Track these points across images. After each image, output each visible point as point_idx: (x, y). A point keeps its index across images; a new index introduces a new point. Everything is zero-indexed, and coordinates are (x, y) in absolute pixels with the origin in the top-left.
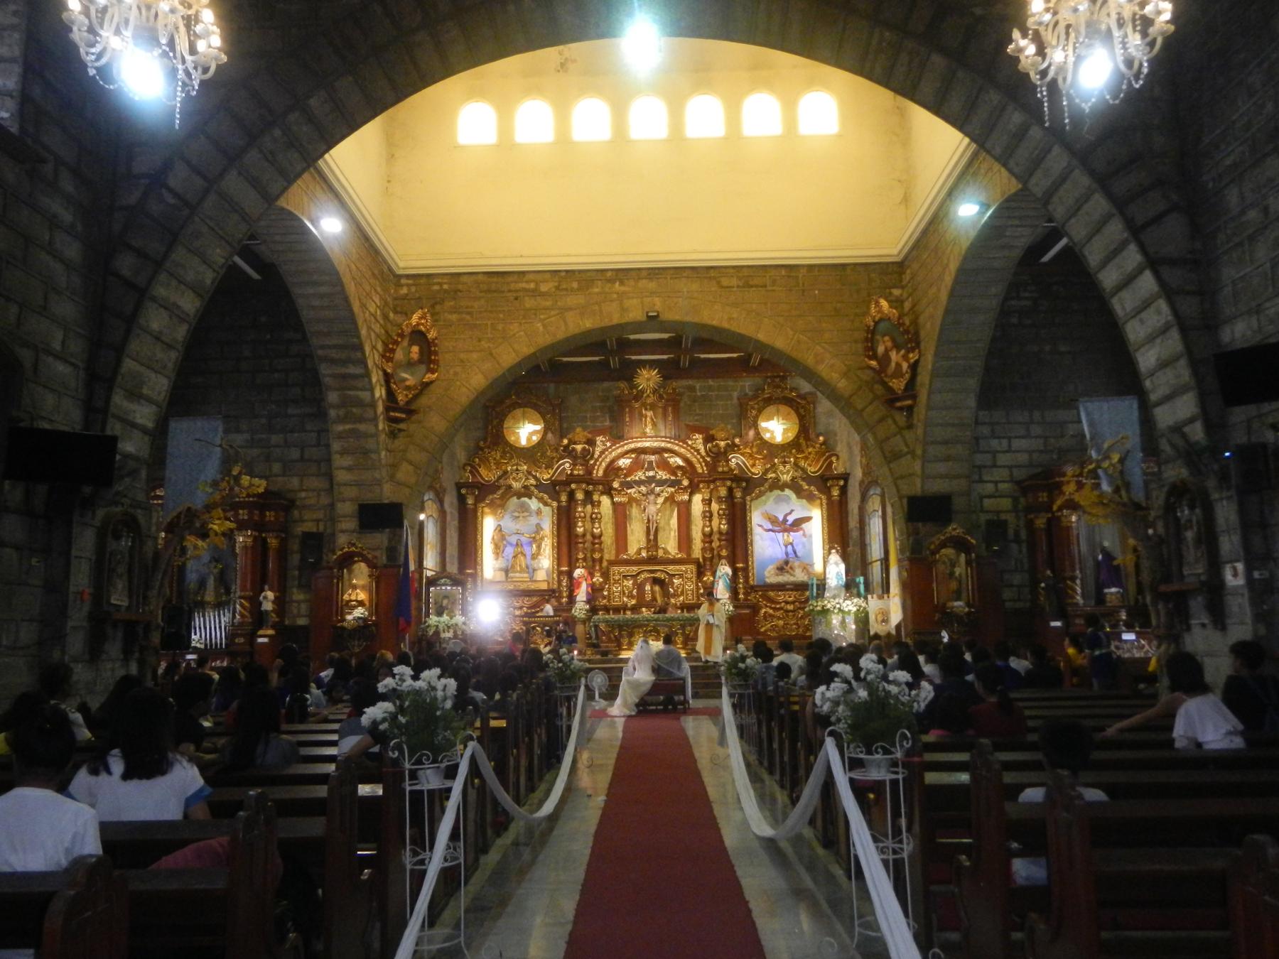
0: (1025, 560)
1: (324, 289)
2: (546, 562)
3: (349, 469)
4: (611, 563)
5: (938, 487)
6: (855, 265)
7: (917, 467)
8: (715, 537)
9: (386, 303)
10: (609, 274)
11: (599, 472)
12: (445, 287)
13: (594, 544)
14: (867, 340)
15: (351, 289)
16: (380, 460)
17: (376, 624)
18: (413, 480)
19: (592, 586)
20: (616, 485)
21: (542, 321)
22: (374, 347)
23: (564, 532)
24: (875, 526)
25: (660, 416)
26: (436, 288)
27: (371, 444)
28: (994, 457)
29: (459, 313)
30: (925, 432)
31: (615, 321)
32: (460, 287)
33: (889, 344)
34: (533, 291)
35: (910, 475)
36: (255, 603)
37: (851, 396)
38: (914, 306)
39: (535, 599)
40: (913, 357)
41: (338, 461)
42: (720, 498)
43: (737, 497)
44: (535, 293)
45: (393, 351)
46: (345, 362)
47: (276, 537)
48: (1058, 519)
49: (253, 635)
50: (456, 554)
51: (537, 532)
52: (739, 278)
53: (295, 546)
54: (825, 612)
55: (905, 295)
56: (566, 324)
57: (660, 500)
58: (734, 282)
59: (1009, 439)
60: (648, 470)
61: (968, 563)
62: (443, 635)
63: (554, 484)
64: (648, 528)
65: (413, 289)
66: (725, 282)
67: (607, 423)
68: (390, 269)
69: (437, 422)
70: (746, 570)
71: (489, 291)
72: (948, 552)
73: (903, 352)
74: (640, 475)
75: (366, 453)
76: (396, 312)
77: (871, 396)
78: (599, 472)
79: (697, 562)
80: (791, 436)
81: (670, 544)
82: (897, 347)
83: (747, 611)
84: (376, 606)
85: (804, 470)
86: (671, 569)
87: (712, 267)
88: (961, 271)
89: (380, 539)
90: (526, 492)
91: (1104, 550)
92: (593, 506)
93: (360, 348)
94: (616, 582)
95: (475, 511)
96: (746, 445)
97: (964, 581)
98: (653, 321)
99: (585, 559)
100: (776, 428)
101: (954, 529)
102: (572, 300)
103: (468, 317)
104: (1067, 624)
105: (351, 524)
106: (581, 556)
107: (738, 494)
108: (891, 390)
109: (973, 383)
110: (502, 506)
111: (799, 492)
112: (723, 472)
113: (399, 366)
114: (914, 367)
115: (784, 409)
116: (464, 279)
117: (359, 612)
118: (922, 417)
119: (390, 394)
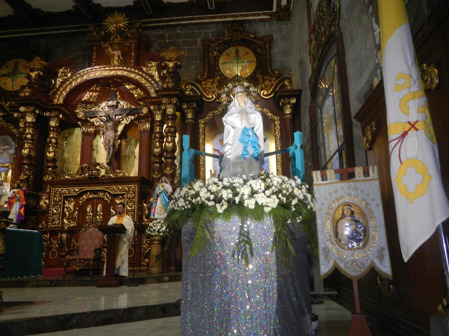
11: (59, 100)
57: (120, 128)
80: (248, 72)
115: (242, 50)
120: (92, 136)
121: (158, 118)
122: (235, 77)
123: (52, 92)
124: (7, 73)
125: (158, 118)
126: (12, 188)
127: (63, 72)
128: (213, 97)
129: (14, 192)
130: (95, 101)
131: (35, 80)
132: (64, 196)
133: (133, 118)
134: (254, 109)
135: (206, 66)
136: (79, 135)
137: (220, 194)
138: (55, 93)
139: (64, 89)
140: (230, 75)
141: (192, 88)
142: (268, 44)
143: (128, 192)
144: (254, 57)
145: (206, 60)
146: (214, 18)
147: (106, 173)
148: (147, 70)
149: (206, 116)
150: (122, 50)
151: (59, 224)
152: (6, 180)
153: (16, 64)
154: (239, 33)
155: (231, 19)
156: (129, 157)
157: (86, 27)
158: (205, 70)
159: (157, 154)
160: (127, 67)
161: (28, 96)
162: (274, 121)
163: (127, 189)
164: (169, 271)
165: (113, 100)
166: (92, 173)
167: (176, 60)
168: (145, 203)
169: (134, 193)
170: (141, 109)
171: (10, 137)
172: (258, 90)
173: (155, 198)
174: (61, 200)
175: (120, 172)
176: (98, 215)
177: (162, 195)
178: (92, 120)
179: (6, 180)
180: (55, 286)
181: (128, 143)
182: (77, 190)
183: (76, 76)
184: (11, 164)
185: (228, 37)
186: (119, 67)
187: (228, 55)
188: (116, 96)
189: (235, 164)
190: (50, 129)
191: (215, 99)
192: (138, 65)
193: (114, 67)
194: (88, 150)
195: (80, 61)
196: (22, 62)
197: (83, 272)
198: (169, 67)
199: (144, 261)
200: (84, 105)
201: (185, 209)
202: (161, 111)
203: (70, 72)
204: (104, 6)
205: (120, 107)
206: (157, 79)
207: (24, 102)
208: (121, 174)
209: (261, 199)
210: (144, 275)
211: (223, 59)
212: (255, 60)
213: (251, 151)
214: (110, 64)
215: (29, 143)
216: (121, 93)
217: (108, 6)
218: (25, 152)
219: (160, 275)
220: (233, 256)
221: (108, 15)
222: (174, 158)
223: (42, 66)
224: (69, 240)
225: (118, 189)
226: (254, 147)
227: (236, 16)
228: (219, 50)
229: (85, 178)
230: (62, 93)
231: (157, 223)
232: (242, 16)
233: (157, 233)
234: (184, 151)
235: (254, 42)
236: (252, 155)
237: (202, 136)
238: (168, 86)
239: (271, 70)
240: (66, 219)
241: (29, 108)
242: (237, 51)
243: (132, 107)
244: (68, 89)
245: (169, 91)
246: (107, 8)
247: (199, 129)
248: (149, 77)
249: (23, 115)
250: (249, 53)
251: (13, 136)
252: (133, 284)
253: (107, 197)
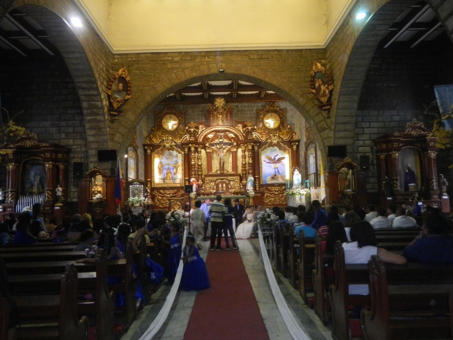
0: (376, 172)
1: (77, 55)
2: (179, 176)
3: (93, 136)
4: (206, 176)
5: (341, 142)
6: (306, 49)
7: (332, 134)
8: (247, 165)
9: (108, 65)
10: (203, 53)
11: (200, 140)
12: (134, 59)
13: (198, 168)
14: (311, 81)
15: (90, 55)
16: (106, 132)
17: (106, 201)
18: (121, 140)
19: (198, 185)
20: (207, 145)
21: (174, 73)
22: (102, 83)
23: (187, 164)
24: (312, 160)
25: (225, 117)
26: (130, 59)
27: (102, 125)
28: (364, 130)
29: (140, 70)
30: (336, 119)
31: (206, 73)
32: (140, 59)
33: (321, 82)
34: (171, 60)
35: (329, 137)
36: (54, 192)
37: (304, 105)
38: (331, 66)
39: (175, 191)
40: (331, 87)
41: (89, 132)
42: (249, 150)
43: (256, 149)
44: (172, 61)
45: (111, 85)
46: (89, 89)
47: (63, 165)
48: (390, 155)
49: (53, 206)
50: (143, 173)
51: (176, 164)
52: (258, 55)
53: (71, 168)
54: (293, 194)
55: (327, 62)
56: (185, 75)
57: (225, 151)
58: (256, 57)
59: (370, 122)
60: (220, 139)
61: (353, 174)
62: (135, 205)
63: (183, 144)
64: (220, 162)
65: (120, 60)
66: (252, 57)
67: (204, 121)
68: (110, 51)
69: (131, 116)
70: (259, 178)
71: (153, 61)
72: (344, 169)
73: (326, 85)
74: (217, 141)
75: (100, 129)
76: (113, 70)
77: (313, 105)
78: (200, 140)
79: (239, 175)
80: (277, 125)
81: (229, 168)
82: (324, 83)
83: (260, 195)
84: (106, 193)
85: (282, 139)
86: (230, 178)
87: (246, 51)
88: (355, 47)
89: (107, 165)
90: (171, 148)
91: (408, 168)
92: (198, 153)
93: (95, 82)
94: (207, 183)
95: (151, 155)
96: (259, 129)
97: (351, 181)
98: (222, 75)
99: (195, 174)
100: (271, 122)
101: (348, 159)
102: (187, 65)
103: (143, 72)
104: (394, 199)
105: (95, 159)
106: (193, 173)
107: (256, 148)
108: (321, 102)
109: (356, 98)
110: (162, 154)
111: (280, 148)
112: (250, 139)
113: (114, 92)
114: (331, 92)
115: (274, 114)
116: (142, 55)
117: (98, 196)
118: (334, 113)
119: (110, 104)
138: (199, 136)
143: (235, 179)
206: (242, 132)
209: (304, 192)
242: (272, 115)
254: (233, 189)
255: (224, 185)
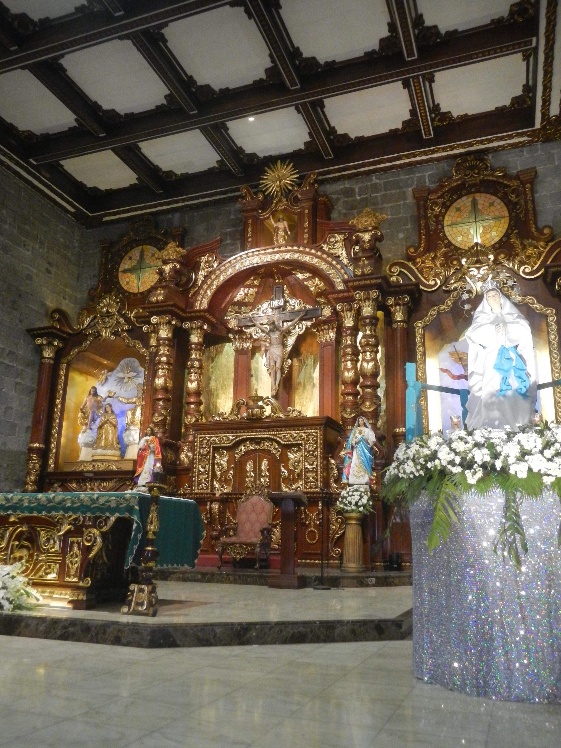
11: (202, 303)
57: (291, 341)
80: (496, 235)
100: (474, 230)
112: (363, 274)
120: (250, 354)
121: (349, 323)
122: (473, 247)
123: (192, 292)
124: (130, 267)
125: (349, 323)
126: (143, 434)
127: (206, 262)
128: (436, 284)
129: (147, 441)
130: (252, 301)
131: (170, 276)
132: (214, 447)
133: (309, 324)
134: (516, 315)
135: (423, 232)
136: (230, 354)
137: (470, 455)
138: (197, 293)
139: (209, 286)
140: (464, 243)
141: (401, 272)
142: (528, 185)
144: (505, 208)
145: (423, 222)
146: (433, 152)
147: (272, 412)
148: (329, 249)
149: (427, 315)
150: (289, 219)
151: (207, 489)
152: (133, 423)
153: (142, 253)
154: (476, 171)
155: (462, 150)
156: (304, 385)
157: (237, 190)
158: (420, 239)
159: (349, 381)
160: (299, 247)
161: (162, 301)
162: (546, 316)
163: (304, 436)
164: (374, 569)
165: (279, 299)
166: (252, 412)
167: (375, 228)
168: (333, 457)
169: (316, 443)
170: (322, 309)
171: (136, 360)
172: (514, 266)
173: (349, 450)
174: (209, 452)
175: (294, 411)
176: (263, 476)
177: (359, 446)
178: (248, 331)
179: (133, 423)
180: (209, 581)
181: (302, 363)
182: (231, 438)
183: (224, 265)
184: (139, 398)
185: (457, 180)
186: (286, 247)
187: (458, 210)
188: (283, 291)
189: (489, 406)
190: (192, 348)
191: (440, 286)
192: (315, 240)
193: (280, 247)
194: (243, 376)
195: (228, 242)
196: (150, 250)
197: (246, 563)
198: (364, 241)
199: (333, 551)
200: (236, 308)
201: (415, 476)
202: (353, 312)
203: (216, 260)
204: (261, 155)
205: (289, 308)
206: (345, 261)
207: (156, 309)
208: (295, 414)
209: (537, 463)
210: (334, 573)
211: (451, 218)
212: (507, 214)
213: (515, 383)
214: (273, 244)
215: (163, 369)
216: (290, 287)
217: (267, 154)
218: (159, 382)
219: (361, 575)
220: (495, 551)
221: (266, 168)
222: (376, 386)
223: (179, 256)
224: (222, 512)
225: (291, 436)
226: (520, 377)
227: (471, 145)
228: (444, 204)
229: (242, 420)
230: (206, 292)
231: (353, 492)
232: (482, 142)
233: (354, 508)
234: (409, 388)
235: (503, 183)
236: (516, 390)
237: (421, 349)
238: (363, 272)
239: (536, 228)
240: (218, 481)
241: (162, 318)
242: (474, 203)
243: (309, 307)
244: (214, 287)
245: (365, 280)
246: (265, 157)
247: (415, 337)
248: (333, 260)
249: (154, 327)
250: (496, 204)
251: (141, 359)
252: (322, 587)
253: (275, 449)
254: (295, 481)
255: (264, 465)
